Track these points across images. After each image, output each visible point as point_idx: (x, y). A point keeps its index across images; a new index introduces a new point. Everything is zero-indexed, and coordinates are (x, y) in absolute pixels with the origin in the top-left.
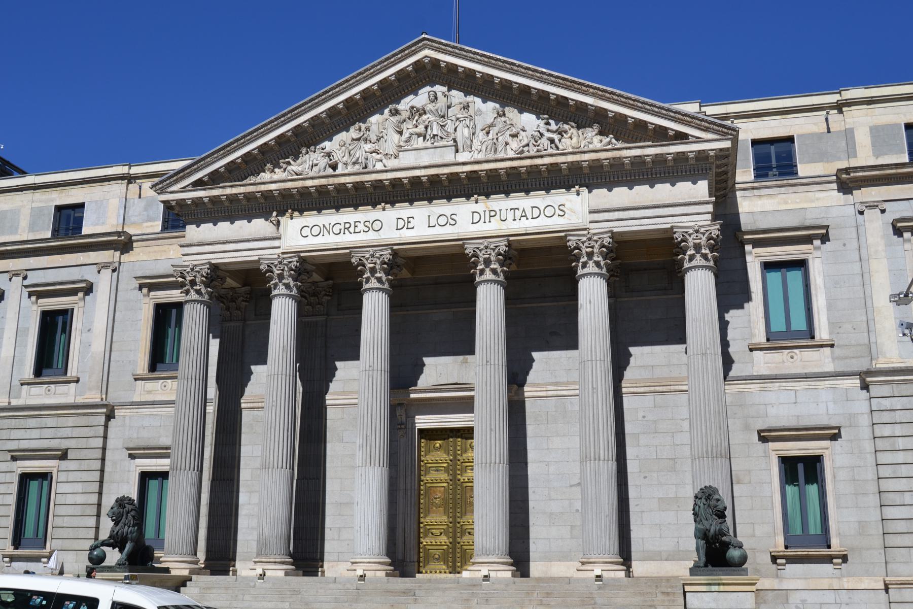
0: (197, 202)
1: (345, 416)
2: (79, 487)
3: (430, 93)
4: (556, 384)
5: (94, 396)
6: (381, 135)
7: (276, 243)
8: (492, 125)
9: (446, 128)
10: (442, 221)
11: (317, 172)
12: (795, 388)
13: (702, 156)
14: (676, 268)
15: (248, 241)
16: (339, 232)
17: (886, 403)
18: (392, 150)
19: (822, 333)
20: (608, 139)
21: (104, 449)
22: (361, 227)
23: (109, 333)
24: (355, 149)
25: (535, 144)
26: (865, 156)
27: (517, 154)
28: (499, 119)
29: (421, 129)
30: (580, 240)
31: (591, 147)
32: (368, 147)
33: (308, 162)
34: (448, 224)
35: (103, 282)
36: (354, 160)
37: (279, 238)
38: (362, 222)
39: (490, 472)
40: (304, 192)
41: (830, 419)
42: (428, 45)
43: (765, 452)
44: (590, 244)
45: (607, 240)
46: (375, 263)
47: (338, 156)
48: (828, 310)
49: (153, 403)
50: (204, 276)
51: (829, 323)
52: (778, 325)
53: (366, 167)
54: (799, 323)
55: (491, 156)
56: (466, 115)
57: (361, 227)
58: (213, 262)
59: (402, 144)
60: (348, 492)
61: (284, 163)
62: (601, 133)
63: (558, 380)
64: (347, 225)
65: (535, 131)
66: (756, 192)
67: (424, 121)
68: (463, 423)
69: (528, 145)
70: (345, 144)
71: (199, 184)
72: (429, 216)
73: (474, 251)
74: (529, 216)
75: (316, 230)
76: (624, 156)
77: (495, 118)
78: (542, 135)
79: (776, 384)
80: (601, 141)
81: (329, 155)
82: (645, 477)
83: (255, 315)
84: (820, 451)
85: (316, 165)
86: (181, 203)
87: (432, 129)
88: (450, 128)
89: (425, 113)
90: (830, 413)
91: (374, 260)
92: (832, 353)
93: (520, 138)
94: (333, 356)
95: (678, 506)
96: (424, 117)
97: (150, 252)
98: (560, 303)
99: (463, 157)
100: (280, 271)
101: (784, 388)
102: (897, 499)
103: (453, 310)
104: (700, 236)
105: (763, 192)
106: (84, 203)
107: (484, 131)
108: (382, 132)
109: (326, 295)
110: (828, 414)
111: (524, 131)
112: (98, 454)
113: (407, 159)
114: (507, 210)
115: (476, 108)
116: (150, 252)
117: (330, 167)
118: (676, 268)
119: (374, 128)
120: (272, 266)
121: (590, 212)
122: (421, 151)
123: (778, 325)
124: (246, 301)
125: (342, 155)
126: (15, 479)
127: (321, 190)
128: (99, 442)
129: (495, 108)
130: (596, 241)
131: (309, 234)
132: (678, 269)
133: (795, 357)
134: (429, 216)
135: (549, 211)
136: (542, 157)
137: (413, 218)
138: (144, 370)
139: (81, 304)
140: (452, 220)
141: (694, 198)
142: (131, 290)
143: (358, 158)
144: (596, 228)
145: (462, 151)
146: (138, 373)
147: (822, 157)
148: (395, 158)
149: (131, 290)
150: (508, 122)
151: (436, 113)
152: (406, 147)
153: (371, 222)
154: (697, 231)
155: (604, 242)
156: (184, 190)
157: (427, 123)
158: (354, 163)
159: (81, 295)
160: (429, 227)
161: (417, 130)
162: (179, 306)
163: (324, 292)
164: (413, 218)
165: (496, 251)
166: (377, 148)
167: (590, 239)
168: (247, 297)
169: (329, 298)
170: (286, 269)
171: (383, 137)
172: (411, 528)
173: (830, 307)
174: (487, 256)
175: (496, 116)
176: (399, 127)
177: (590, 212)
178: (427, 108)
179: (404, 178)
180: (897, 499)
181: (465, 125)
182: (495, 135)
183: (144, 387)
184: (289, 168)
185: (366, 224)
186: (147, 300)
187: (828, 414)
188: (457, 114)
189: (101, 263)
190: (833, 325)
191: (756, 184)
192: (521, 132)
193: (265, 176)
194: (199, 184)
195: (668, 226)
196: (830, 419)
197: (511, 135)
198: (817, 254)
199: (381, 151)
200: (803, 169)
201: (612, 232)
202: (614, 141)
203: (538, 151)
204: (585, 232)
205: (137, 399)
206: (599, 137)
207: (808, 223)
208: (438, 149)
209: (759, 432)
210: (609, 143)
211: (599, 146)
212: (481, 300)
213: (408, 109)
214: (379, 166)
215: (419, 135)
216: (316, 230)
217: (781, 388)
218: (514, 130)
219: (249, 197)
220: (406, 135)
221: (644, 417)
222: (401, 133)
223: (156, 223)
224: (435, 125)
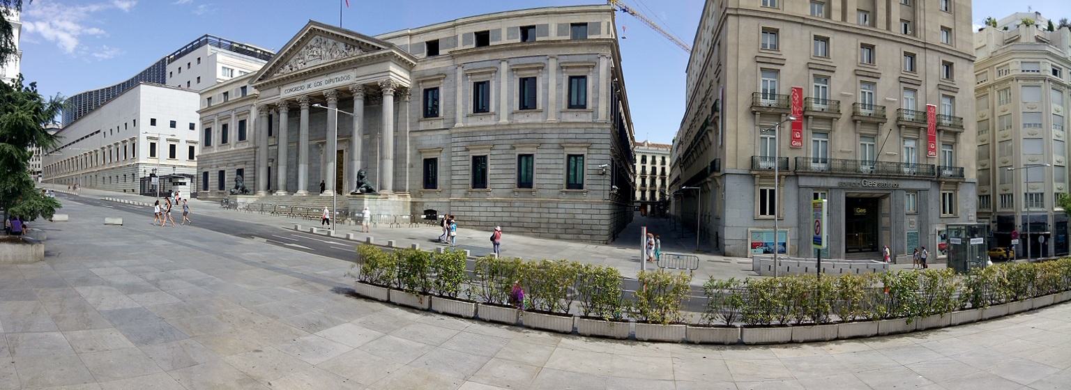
2: (250, 172)
13: (385, 55)
17: (456, 139)
19: (441, 114)
21: (255, 161)
26: (460, 47)
29: (312, 54)
62: (360, 48)
71: (260, 80)
79: (426, 133)
99: (322, 62)
102: (456, 173)
113: (308, 65)
126: (235, 170)
127: (287, 78)
140: (320, 84)
147: (447, 47)
173: (444, 104)
180: (456, 173)
193: (275, 75)
194: (260, 80)
200: (441, 52)
219: (271, 82)
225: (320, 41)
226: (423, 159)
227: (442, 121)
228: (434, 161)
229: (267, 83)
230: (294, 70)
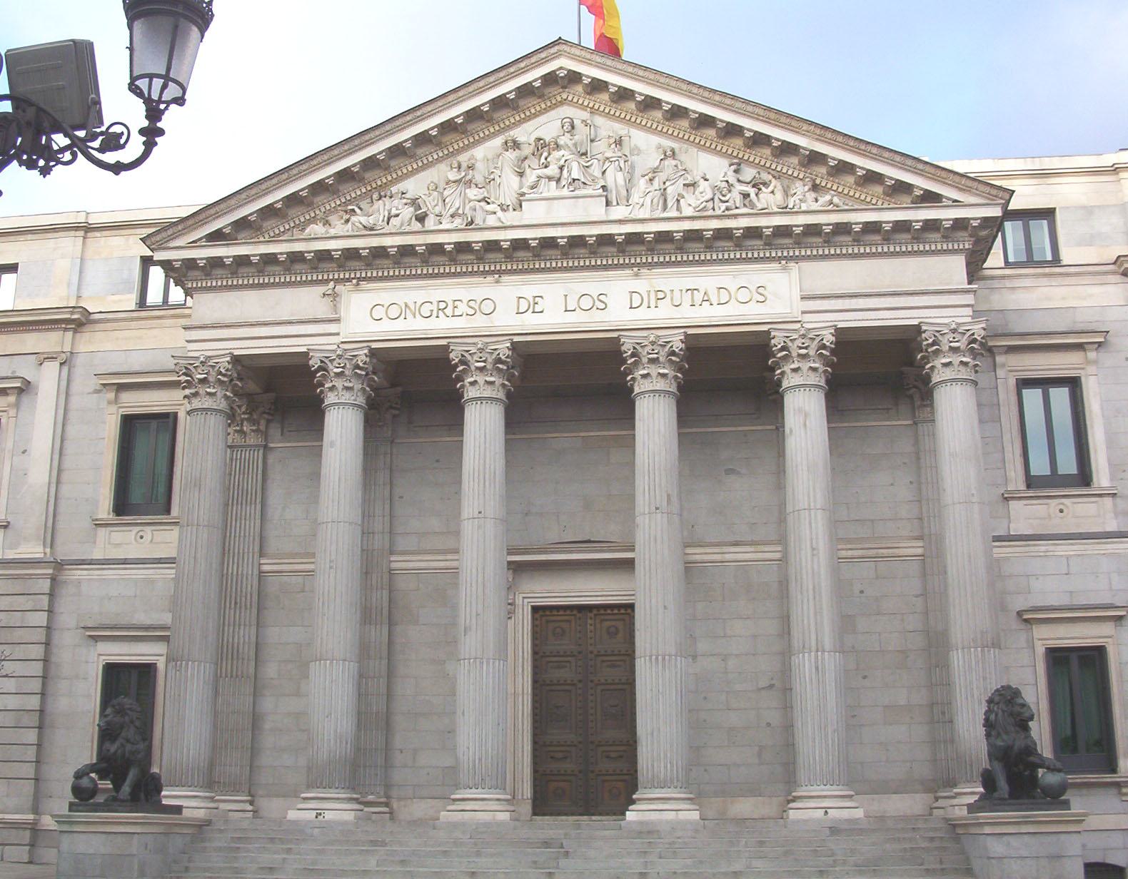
0: (216, 263)
1: (421, 585)
3: (565, 120)
4: (736, 544)
5: (30, 551)
6: (492, 177)
7: (332, 328)
8: (655, 171)
9: (590, 170)
10: (586, 303)
11: (398, 225)
12: (1067, 553)
13: (960, 224)
14: (905, 384)
15: (290, 323)
16: (429, 315)
18: (510, 200)
19: (1102, 476)
20: (828, 197)
22: (462, 308)
23: (56, 457)
24: (454, 195)
25: (723, 199)
27: (698, 211)
28: (666, 162)
29: (553, 170)
30: (787, 337)
31: (804, 207)
32: (473, 193)
33: (381, 211)
34: (595, 308)
35: (48, 380)
36: (452, 211)
37: (337, 320)
38: (465, 301)
39: (664, 666)
40: (379, 252)
41: (1114, 596)
42: (565, 52)
43: (1027, 641)
44: (803, 344)
45: (829, 339)
46: (484, 361)
47: (430, 203)
48: (1107, 448)
49: (125, 562)
50: (220, 373)
51: (1109, 464)
52: (1040, 466)
53: (472, 222)
54: (1068, 465)
55: (659, 214)
56: (620, 155)
57: (462, 308)
58: (237, 353)
59: (524, 190)
60: (427, 698)
61: (346, 212)
62: (815, 188)
63: (738, 538)
64: (442, 305)
65: (722, 181)
66: (1008, 283)
67: (559, 160)
68: (599, 598)
69: (713, 199)
70: (436, 188)
71: (217, 236)
72: (566, 296)
73: (634, 348)
74: (715, 302)
75: (394, 312)
76: (853, 221)
77: (661, 160)
78: (730, 186)
79: (1043, 547)
80: (817, 200)
81: (414, 203)
82: (865, 677)
83: (282, 435)
84: (1101, 640)
85: (397, 215)
86: (190, 264)
87: (570, 172)
88: (596, 170)
89: (558, 147)
90: (1114, 588)
91: (484, 356)
92: (1115, 505)
93: (700, 189)
94: (401, 497)
95: (912, 718)
96: (556, 154)
97: (117, 339)
98: (740, 429)
99: (619, 212)
100: (341, 370)
101: (1051, 553)
103: (582, 434)
104: (958, 337)
105: (1017, 283)
106: (18, 264)
107: (647, 177)
108: (492, 172)
109: (391, 407)
110: (1111, 589)
111: (706, 180)
112: (40, 635)
113: (534, 212)
114: (682, 290)
115: (632, 145)
116: (117, 339)
117: (416, 219)
118: (905, 384)
119: (479, 165)
120: (326, 361)
121: (803, 298)
122: (556, 201)
123: (1040, 466)
124: (268, 414)
125: (433, 204)
127: (407, 251)
128: (41, 619)
129: (659, 147)
130: (812, 339)
131: (383, 316)
132: (908, 384)
133: (1065, 510)
134: (566, 296)
135: (744, 295)
136: (736, 216)
137: (541, 297)
138: (109, 514)
139: (12, 412)
140: (600, 303)
141: (947, 284)
142: (89, 393)
143: (458, 209)
144: (812, 321)
145: (615, 203)
146: (100, 517)
148: (514, 210)
149: (89, 393)
150: (680, 168)
151: (573, 149)
152: (532, 195)
153: (478, 302)
154: (954, 331)
155: (824, 342)
156: (194, 244)
157: (562, 162)
158: (452, 216)
159: (12, 399)
160: (566, 311)
161: (548, 172)
162: (167, 421)
163: (389, 404)
164: (541, 297)
165: (667, 349)
166: (486, 195)
167: (803, 336)
168: (270, 409)
169: (397, 412)
170: (348, 366)
171: (494, 179)
172: (523, 751)
173: (1111, 442)
174: (655, 356)
175: (662, 157)
176: (519, 168)
177: (803, 298)
178: (562, 141)
179: (532, 239)
181: (619, 169)
182: (662, 184)
183: (109, 538)
184: (354, 219)
185: (472, 304)
186: (113, 409)
187: (1111, 589)
188: (605, 152)
189: (43, 353)
190: (1114, 467)
191: (1008, 272)
192: (702, 182)
193: (317, 229)
194: (217, 236)
195: (915, 322)
196: (1114, 596)
197: (684, 185)
198: (1091, 369)
199: (492, 199)
201: (837, 330)
202: (836, 200)
203: (727, 209)
204: (797, 326)
205: (97, 555)
206: (813, 195)
207: (1079, 327)
208: (581, 200)
209: (1019, 614)
210: (831, 203)
211: (815, 206)
212: (646, 417)
213: (532, 140)
214: (491, 221)
215: (550, 178)
216: (394, 312)
217: (1048, 554)
218: (690, 178)
219: (296, 258)
220: (531, 177)
221: (862, 592)
222: (521, 174)
223: (128, 296)
224: (575, 165)
225: (582, 132)
226: (1040, 650)
227: (1108, 501)
228: (1094, 658)
229: (270, 259)
230: (430, 223)
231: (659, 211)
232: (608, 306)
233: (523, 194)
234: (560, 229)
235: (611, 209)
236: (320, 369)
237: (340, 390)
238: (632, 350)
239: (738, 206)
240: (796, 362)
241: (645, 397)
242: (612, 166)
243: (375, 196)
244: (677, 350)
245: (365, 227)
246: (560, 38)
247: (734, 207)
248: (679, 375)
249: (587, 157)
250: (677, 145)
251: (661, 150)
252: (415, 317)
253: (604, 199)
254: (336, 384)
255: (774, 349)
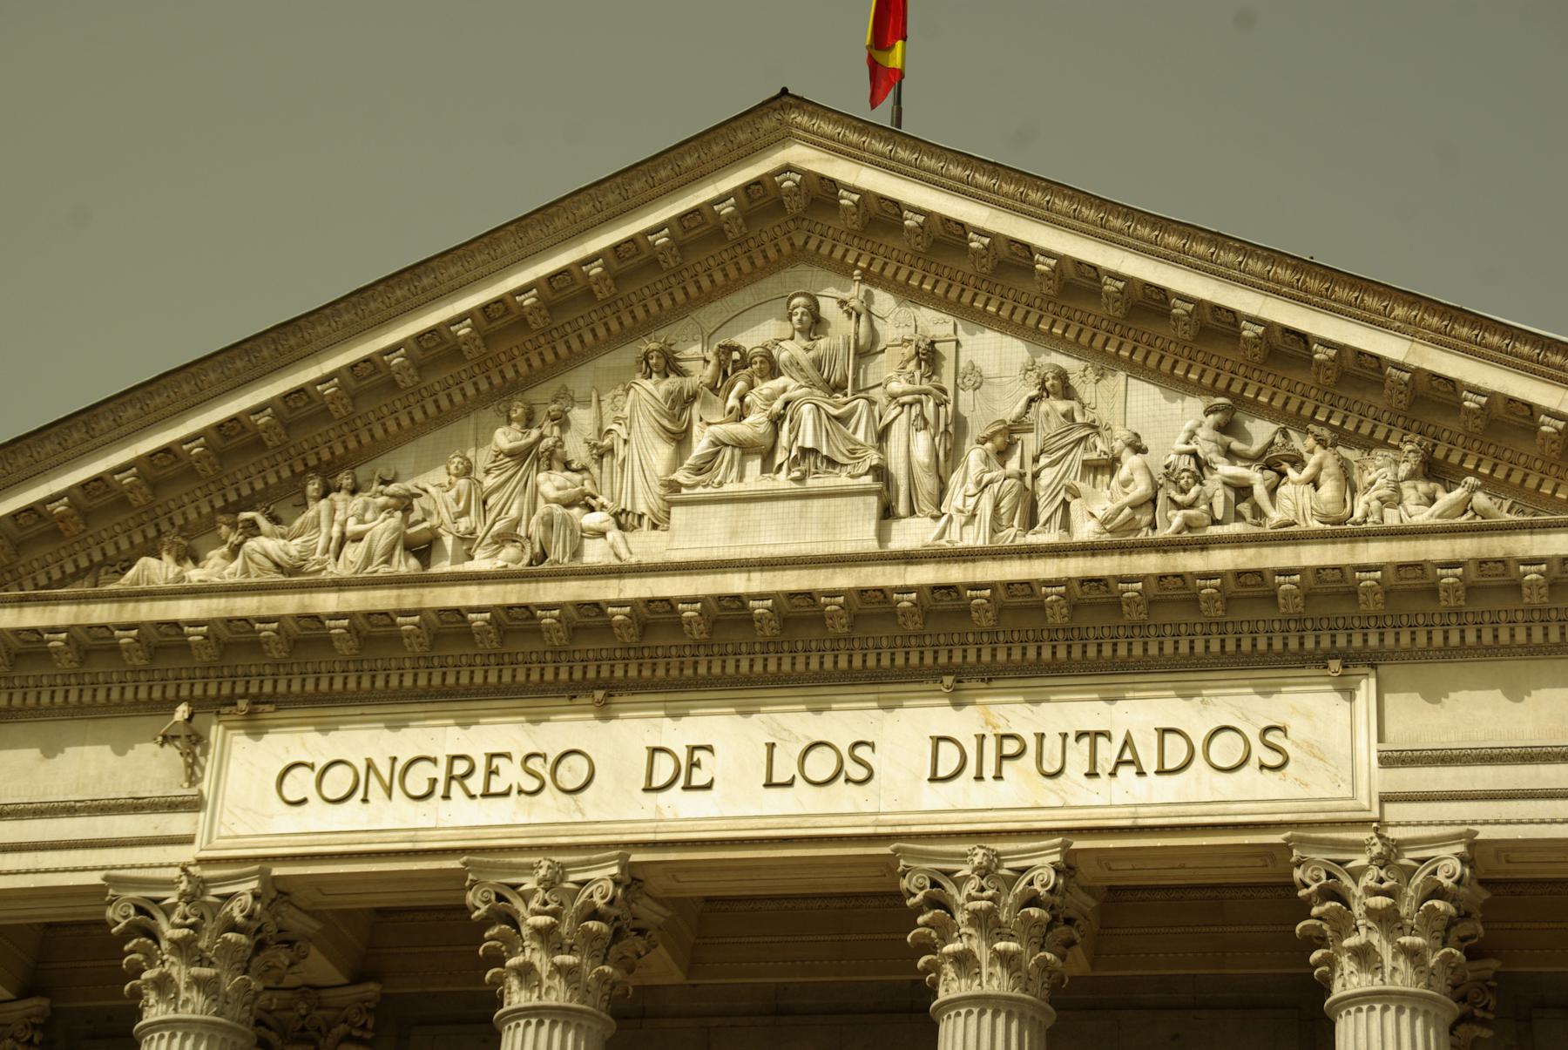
231: (1012, 531)
232: (876, 776)
233: (674, 487)
234: (756, 576)
235: (896, 527)
236: (135, 930)
237: (182, 986)
238: (928, 889)
239: (1219, 515)
240: (1363, 931)
241: (518, 1025)
242: (904, 417)
243: (313, 488)
244: (1042, 891)
245: (277, 565)
246: (784, 91)
247: (1208, 521)
248: (607, 969)
249: (846, 395)
250: (1076, 362)
251: (1034, 375)
252: (390, 797)
253: (873, 501)
254: (174, 971)
255: (1300, 894)
